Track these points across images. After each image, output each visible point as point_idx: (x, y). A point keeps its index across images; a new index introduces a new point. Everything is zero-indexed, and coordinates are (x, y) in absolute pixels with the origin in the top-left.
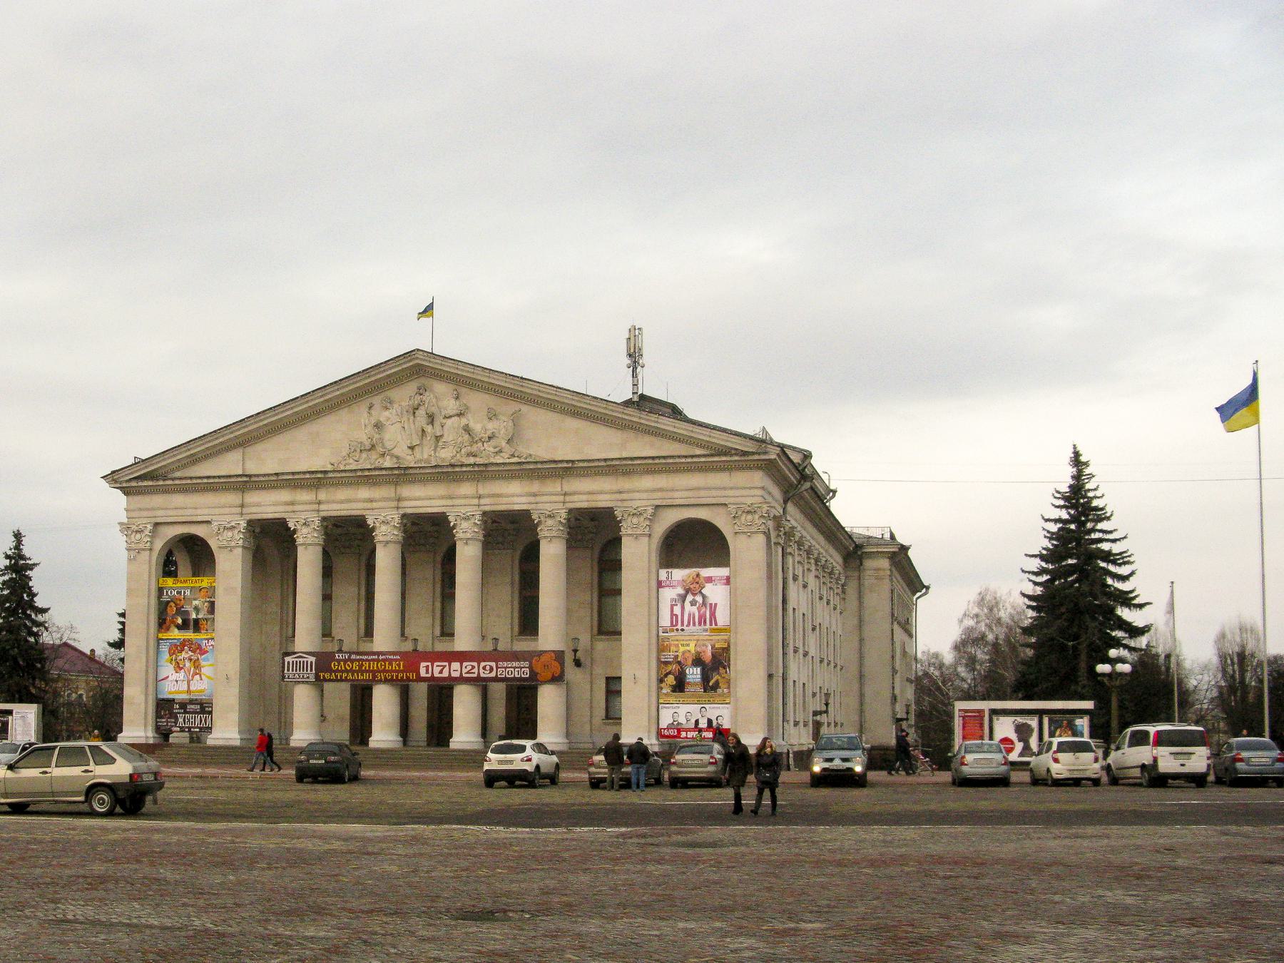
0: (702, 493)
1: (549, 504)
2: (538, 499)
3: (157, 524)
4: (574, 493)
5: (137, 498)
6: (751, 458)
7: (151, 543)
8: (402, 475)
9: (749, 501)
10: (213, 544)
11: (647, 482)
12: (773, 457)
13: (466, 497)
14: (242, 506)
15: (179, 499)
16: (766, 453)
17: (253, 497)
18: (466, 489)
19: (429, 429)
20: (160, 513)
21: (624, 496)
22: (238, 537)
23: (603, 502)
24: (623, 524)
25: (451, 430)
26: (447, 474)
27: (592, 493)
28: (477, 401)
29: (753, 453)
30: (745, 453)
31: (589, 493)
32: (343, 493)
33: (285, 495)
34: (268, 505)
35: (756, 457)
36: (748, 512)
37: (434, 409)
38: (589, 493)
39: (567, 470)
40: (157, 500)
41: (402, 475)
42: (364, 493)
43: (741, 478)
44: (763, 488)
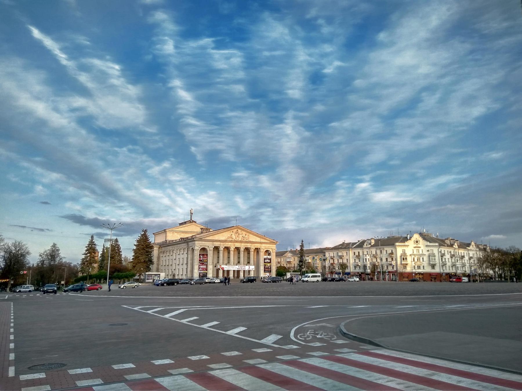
1: (253, 247)
8: (237, 242)
10: (208, 249)
11: (264, 245)
15: (204, 242)
17: (215, 243)
18: (243, 244)
22: (212, 248)
23: (258, 247)
25: (241, 236)
26: (241, 242)
27: (258, 246)
28: (244, 233)
32: (227, 243)
33: (219, 243)
34: (217, 244)
40: (200, 242)
41: (237, 242)
42: (230, 244)
43: (273, 245)
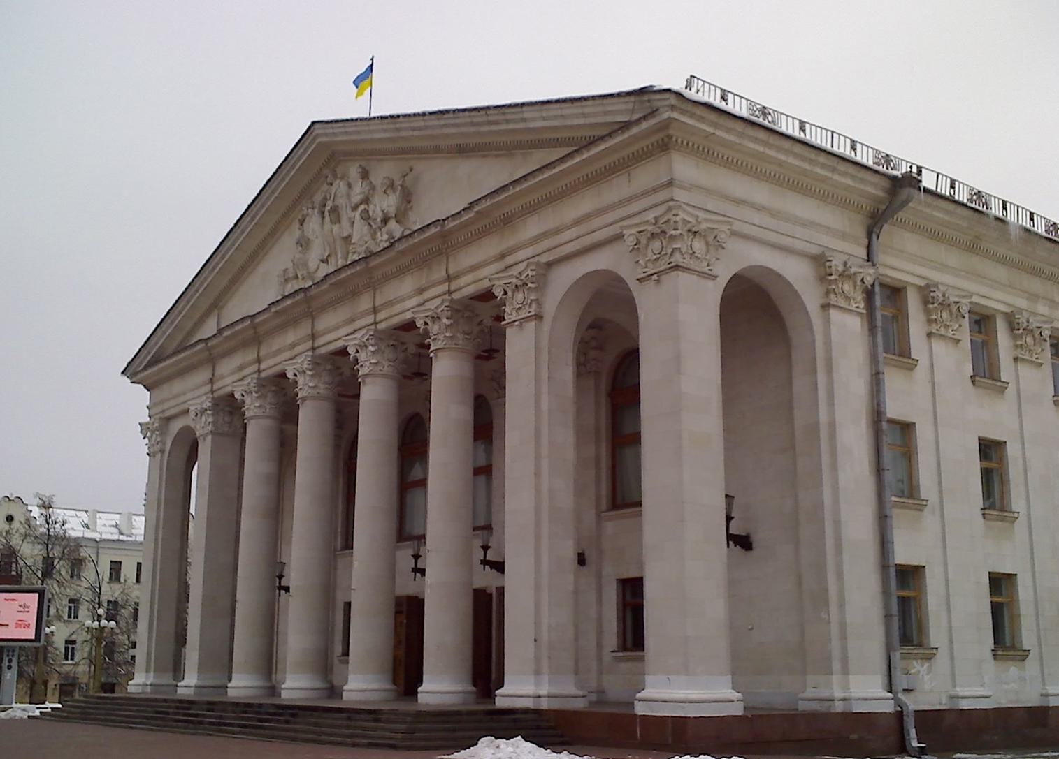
0: (596, 222)
2: (427, 295)
3: (169, 419)
4: (458, 276)
5: (156, 392)
6: (635, 130)
7: (164, 444)
9: (650, 216)
12: (666, 115)
13: (364, 314)
14: (211, 381)
16: (654, 112)
19: (335, 228)
20: (166, 406)
21: (509, 260)
24: (508, 309)
27: (477, 266)
29: (638, 121)
30: (626, 126)
31: (474, 268)
35: (645, 125)
36: (653, 236)
37: (341, 202)
38: (474, 268)
39: (443, 240)
44: (670, 183)
